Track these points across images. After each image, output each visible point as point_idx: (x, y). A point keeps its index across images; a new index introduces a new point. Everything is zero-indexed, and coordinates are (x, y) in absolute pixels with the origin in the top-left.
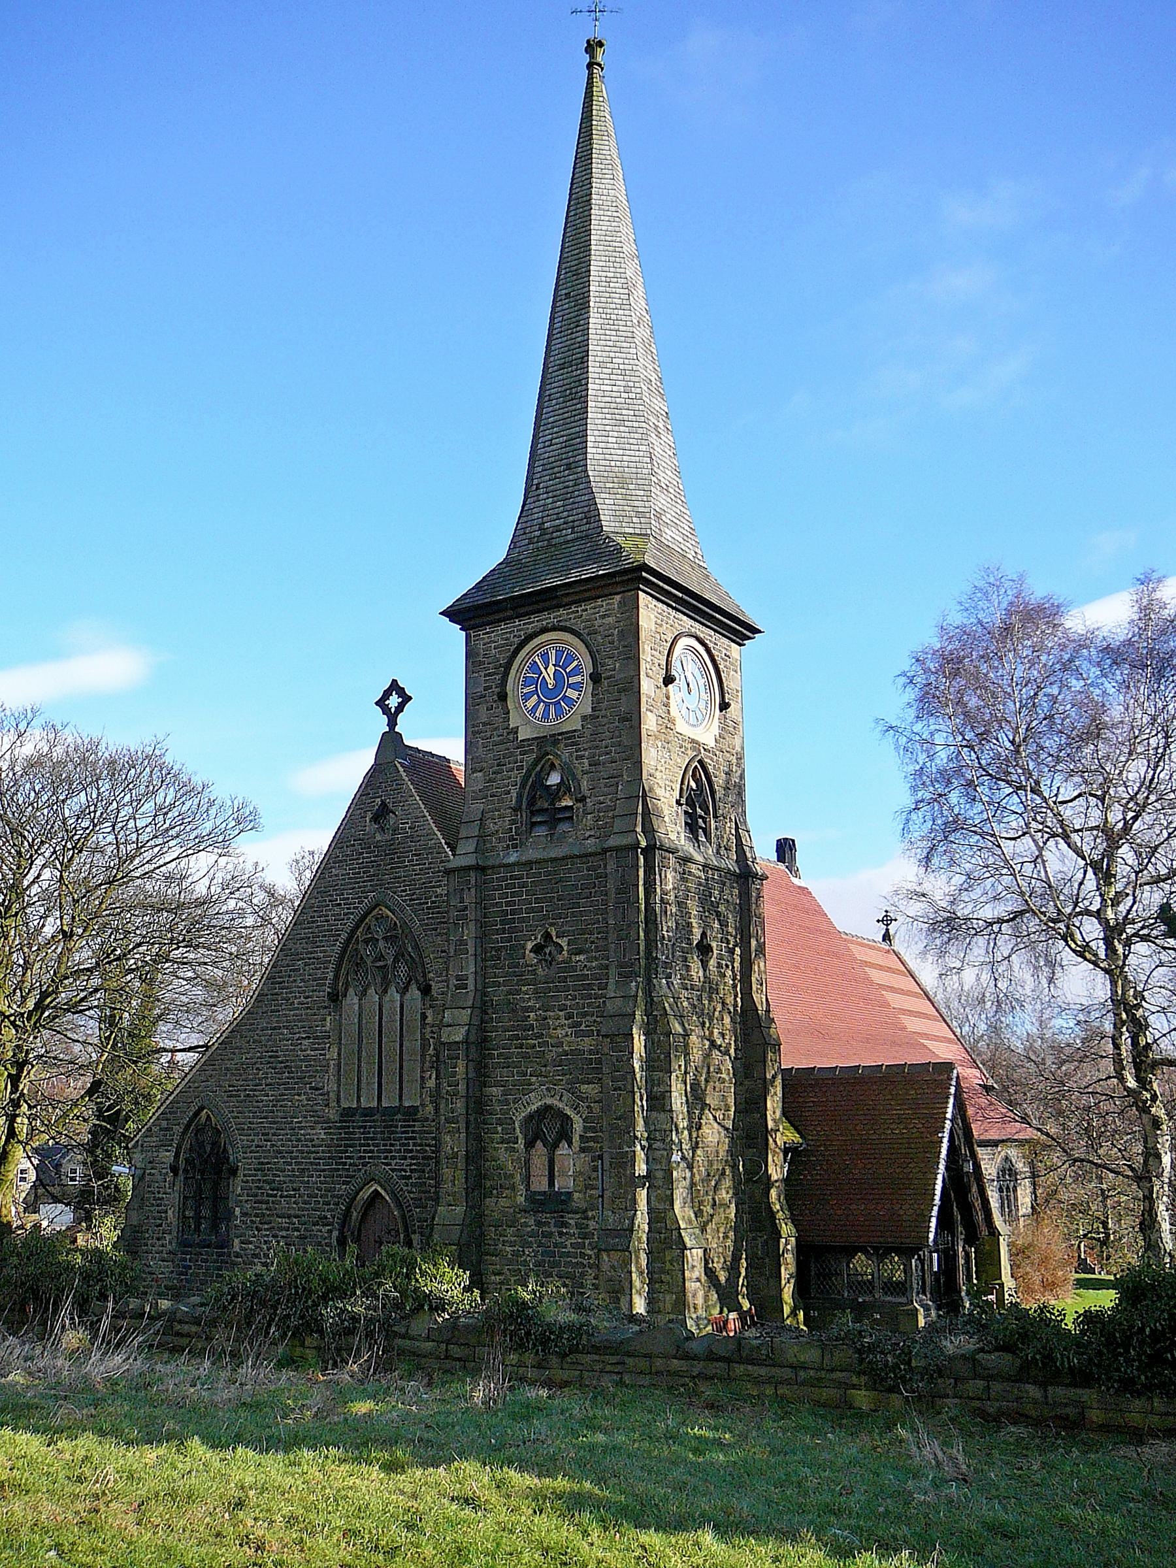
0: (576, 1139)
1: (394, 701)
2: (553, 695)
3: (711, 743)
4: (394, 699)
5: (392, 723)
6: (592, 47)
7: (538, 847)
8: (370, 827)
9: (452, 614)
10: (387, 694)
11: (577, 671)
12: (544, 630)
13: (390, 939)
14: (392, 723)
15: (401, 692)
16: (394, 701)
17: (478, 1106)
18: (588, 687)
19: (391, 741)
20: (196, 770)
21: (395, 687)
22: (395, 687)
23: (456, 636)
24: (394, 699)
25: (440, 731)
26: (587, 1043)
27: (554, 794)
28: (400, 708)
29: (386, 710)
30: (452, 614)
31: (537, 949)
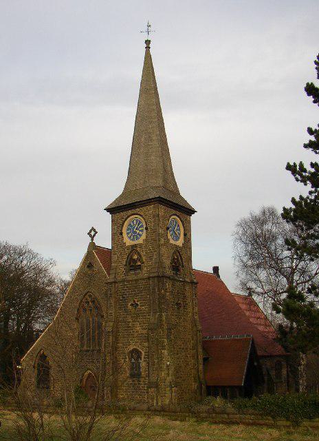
0: (143, 358)
1: (93, 233)
2: (135, 236)
3: (181, 245)
4: (93, 233)
5: (92, 240)
6: (148, 42)
7: (132, 276)
8: (87, 269)
9: (108, 210)
10: (90, 231)
11: (142, 226)
12: (133, 215)
13: (93, 302)
14: (92, 240)
15: (94, 230)
16: (93, 233)
17: (115, 348)
18: (145, 231)
19: (92, 246)
20: (35, 250)
21: (93, 229)
22: (93, 229)
23: (109, 216)
24: (93, 233)
25: (105, 240)
26: (145, 331)
27: (135, 261)
28: (94, 235)
29: (90, 236)
30: (108, 210)
31: (132, 305)
